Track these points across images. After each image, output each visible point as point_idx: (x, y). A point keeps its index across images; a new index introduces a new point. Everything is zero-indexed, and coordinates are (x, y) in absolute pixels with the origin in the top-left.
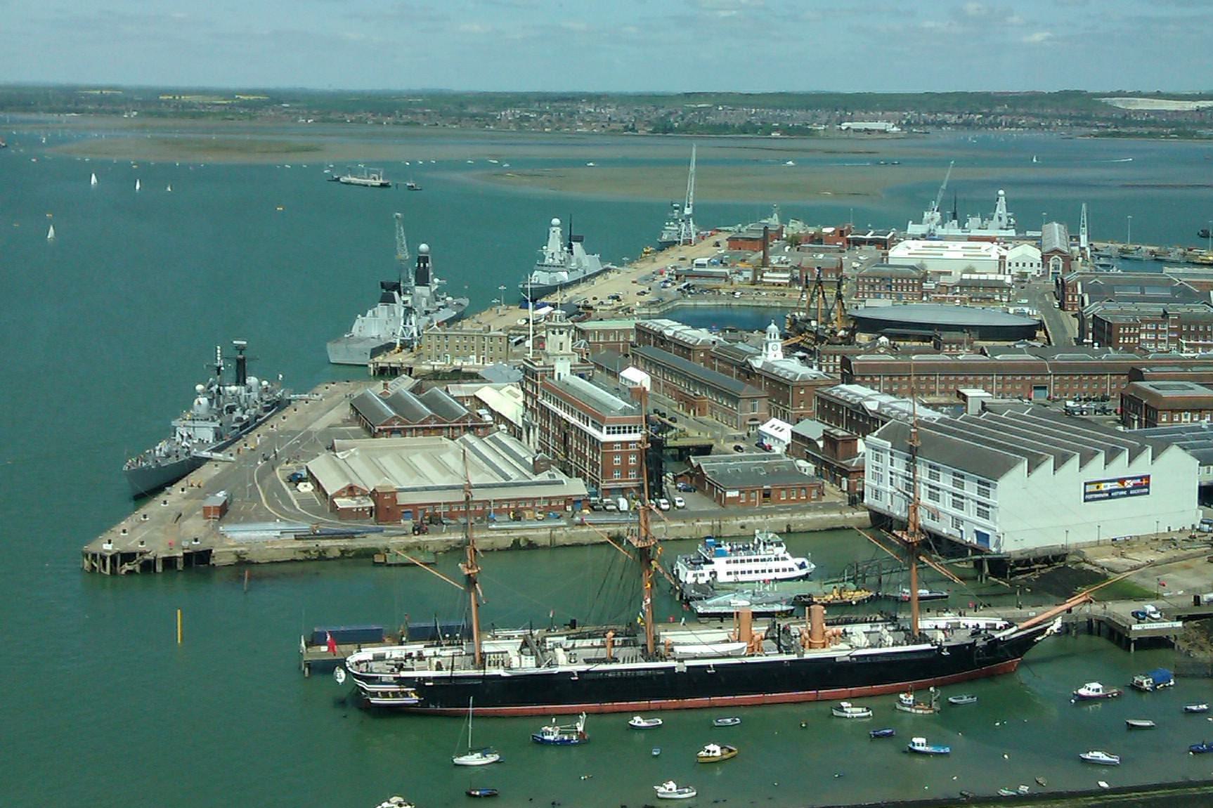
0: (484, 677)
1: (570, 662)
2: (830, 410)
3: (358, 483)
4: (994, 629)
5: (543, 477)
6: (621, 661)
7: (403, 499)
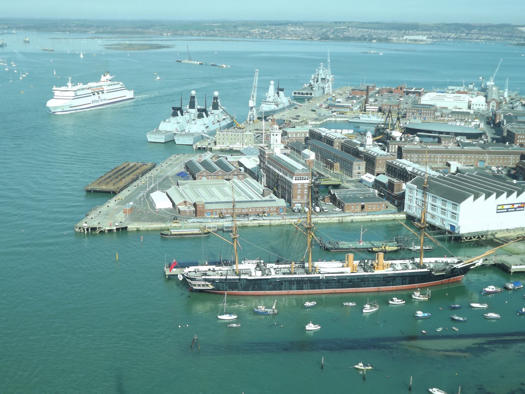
0: (240, 279)
1: (276, 274)
2: (392, 170)
3: (188, 200)
4: (454, 263)
5: (267, 198)
6: (298, 274)
7: (208, 207)
